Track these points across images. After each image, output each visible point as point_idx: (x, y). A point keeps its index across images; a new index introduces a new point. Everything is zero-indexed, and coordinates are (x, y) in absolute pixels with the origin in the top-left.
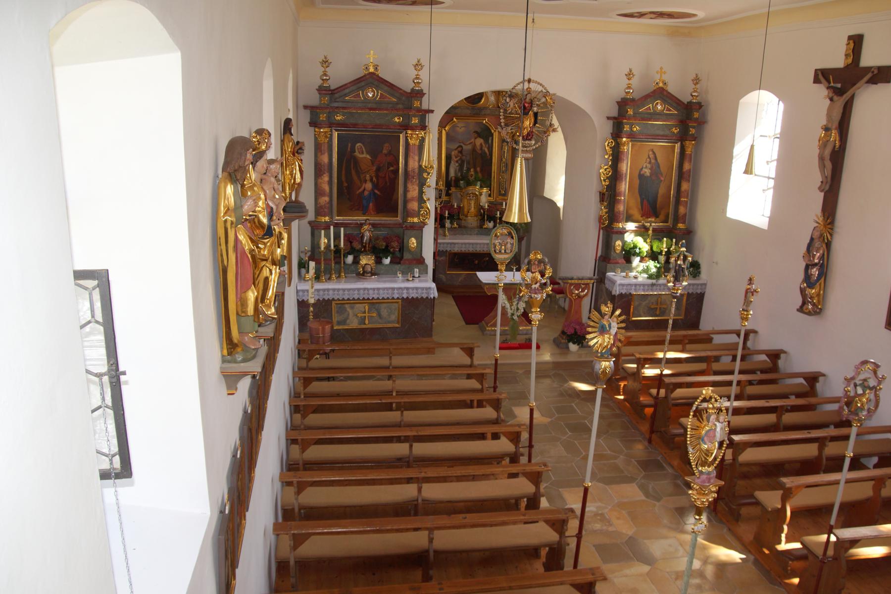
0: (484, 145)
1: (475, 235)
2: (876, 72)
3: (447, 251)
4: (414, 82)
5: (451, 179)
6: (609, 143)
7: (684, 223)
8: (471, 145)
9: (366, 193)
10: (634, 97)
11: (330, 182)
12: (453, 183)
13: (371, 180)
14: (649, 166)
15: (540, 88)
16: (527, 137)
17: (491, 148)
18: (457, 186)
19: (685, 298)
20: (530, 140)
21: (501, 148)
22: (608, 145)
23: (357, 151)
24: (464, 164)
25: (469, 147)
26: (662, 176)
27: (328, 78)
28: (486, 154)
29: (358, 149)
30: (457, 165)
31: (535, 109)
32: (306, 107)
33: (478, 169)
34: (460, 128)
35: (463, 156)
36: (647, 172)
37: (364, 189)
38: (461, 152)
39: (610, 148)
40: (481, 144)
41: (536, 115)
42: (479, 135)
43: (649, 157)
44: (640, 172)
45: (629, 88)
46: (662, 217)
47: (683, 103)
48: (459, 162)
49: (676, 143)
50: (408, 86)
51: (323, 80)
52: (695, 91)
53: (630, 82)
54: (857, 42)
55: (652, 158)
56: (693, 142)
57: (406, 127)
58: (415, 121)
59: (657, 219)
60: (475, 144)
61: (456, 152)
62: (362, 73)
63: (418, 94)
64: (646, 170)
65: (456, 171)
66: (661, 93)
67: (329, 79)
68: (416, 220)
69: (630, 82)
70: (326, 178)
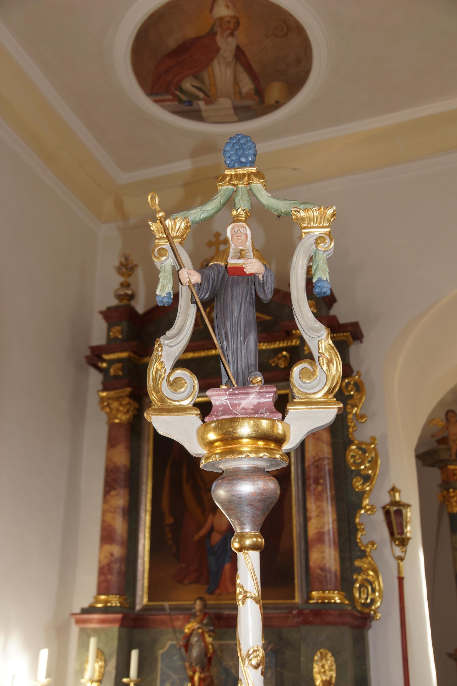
27: (129, 292)
37: (212, 529)
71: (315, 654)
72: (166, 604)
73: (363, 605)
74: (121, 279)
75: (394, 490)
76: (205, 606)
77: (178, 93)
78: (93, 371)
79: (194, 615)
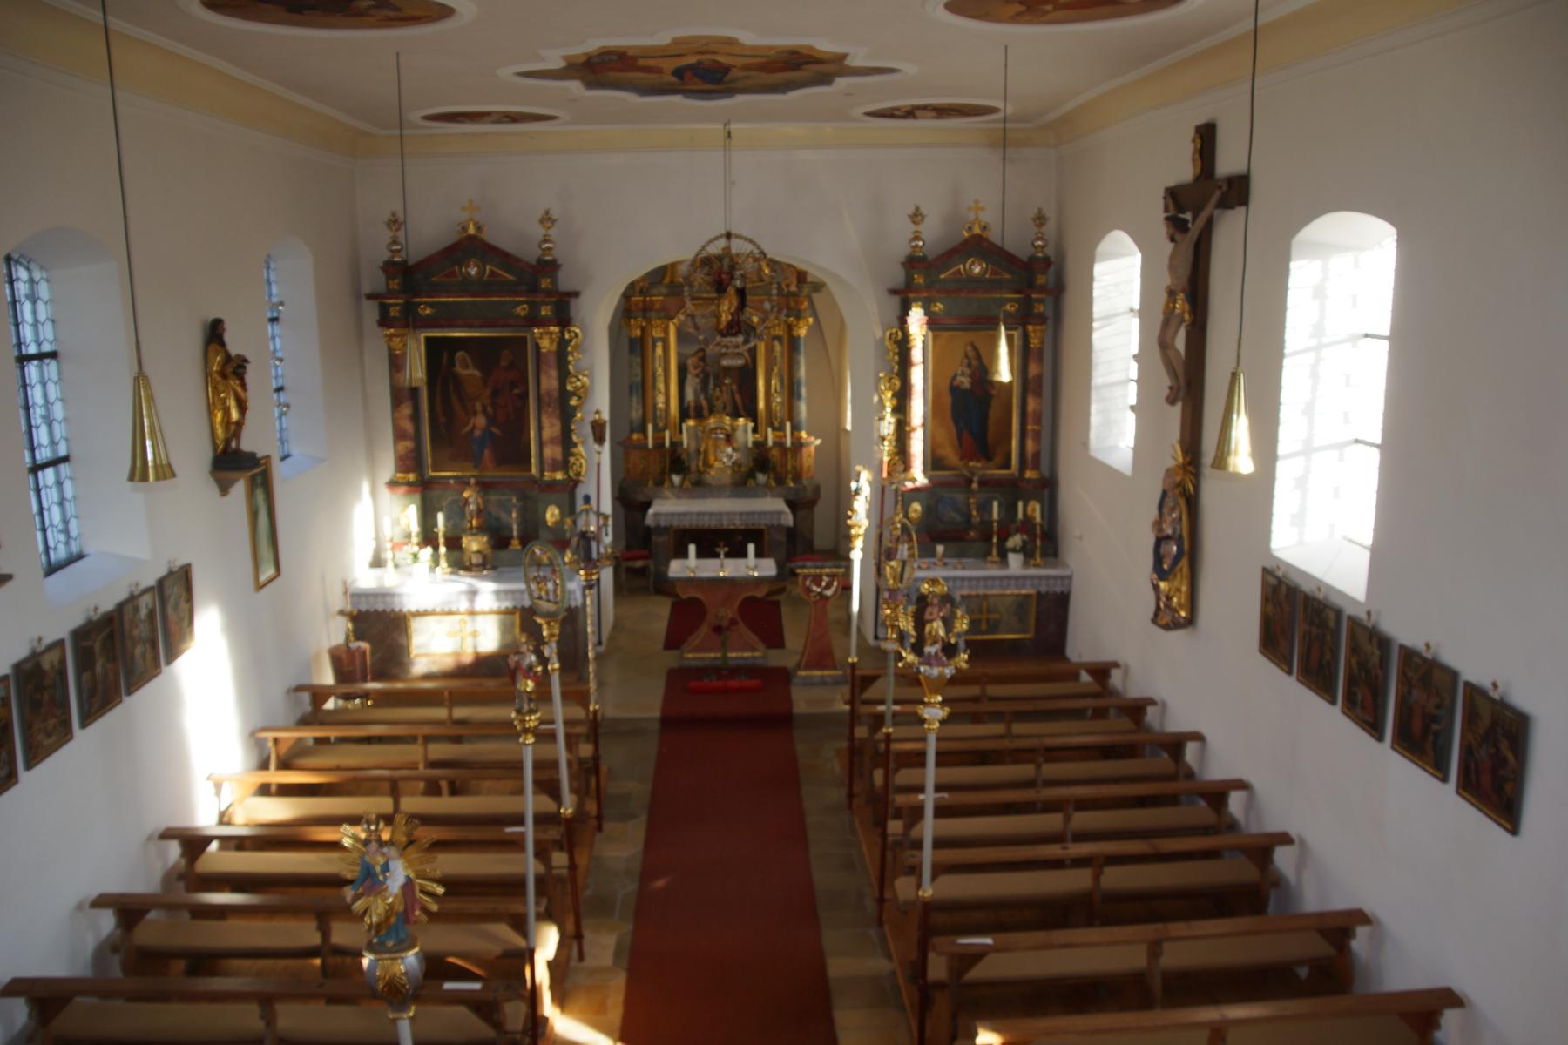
1: (725, 497)
2: (1225, 188)
3: (671, 526)
4: (540, 246)
5: (689, 406)
6: (891, 334)
7: (1036, 466)
9: (478, 433)
11: (415, 417)
12: (692, 412)
13: (484, 412)
15: (748, 248)
16: (727, 331)
18: (699, 415)
19: (1034, 603)
20: (735, 335)
22: (890, 338)
23: (458, 364)
27: (399, 247)
30: (697, 380)
32: (370, 297)
35: (706, 365)
36: (965, 382)
37: (474, 427)
38: (703, 359)
39: (895, 342)
41: (741, 293)
44: (951, 383)
45: (917, 238)
46: (998, 459)
47: (1020, 260)
48: (701, 376)
49: (1015, 329)
50: (531, 254)
51: (392, 251)
52: (1038, 239)
54: (1206, 136)
56: (1038, 327)
57: (534, 320)
58: (545, 311)
62: (453, 238)
63: (548, 266)
65: (696, 394)
66: (977, 245)
68: (559, 476)
69: (920, 228)
70: (406, 410)
74: (391, 234)
75: (598, 412)
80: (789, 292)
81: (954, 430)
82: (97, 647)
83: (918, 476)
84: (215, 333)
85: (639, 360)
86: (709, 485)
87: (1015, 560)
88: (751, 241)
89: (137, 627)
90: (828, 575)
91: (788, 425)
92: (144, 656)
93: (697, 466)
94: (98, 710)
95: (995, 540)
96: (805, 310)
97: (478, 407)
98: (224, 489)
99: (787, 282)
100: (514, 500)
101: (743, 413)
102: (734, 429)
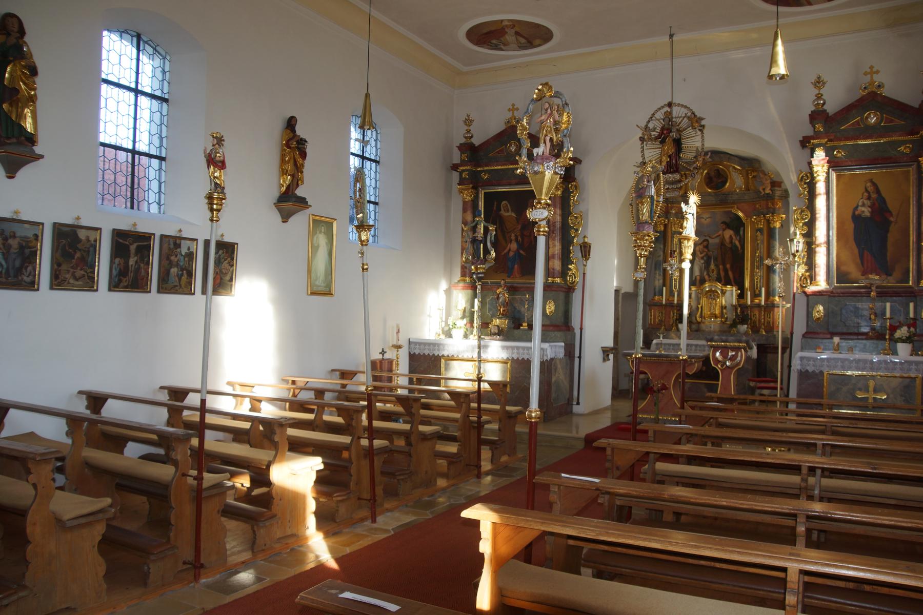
0: (734, 237)
8: (719, 238)
9: (511, 254)
10: (826, 109)
13: (516, 240)
14: (868, 203)
15: (683, 111)
17: (742, 241)
21: (754, 239)
24: (711, 262)
25: (717, 241)
26: (891, 215)
28: (737, 248)
29: (503, 207)
30: (702, 261)
31: (674, 135)
33: (728, 266)
34: (706, 220)
35: (708, 250)
36: (866, 211)
37: (510, 250)
38: (707, 247)
40: (731, 236)
42: (727, 226)
43: (866, 190)
44: (854, 213)
46: (897, 274)
48: (705, 258)
53: (821, 92)
55: (871, 192)
59: (889, 278)
60: (724, 237)
61: (701, 247)
64: (863, 209)
65: (701, 270)
67: (472, 137)
68: (558, 280)
71: (547, 302)
72: (489, 281)
73: (570, 283)
76: (505, 283)
77: (490, 44)
78: (454, 172)
79: (501, 286)
80: (767, 194)
81: (856, 251)
82: (133, 248)
83: (821, 284)
84: (291, 124)
85: (662, 247)
86: (704, 331)
87: (904, 349)
88: (685, 107)
89: (176, 256)
90: (733, 349)
91: (763, 289)
92: (180, 277)
93: (696, 318)
94: (126, 287)
95: (887, 337)
96: (779, 208)
97: (513, 237)
98: (286, 217)
99: (764, 187)
100: (527, 296)
101: (733, 284)
102: (723, 293)
